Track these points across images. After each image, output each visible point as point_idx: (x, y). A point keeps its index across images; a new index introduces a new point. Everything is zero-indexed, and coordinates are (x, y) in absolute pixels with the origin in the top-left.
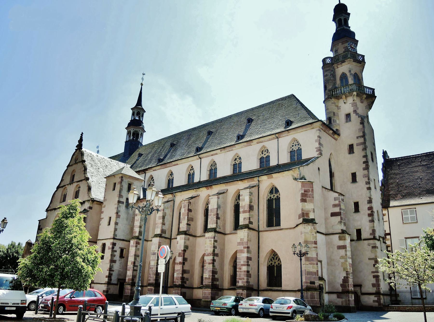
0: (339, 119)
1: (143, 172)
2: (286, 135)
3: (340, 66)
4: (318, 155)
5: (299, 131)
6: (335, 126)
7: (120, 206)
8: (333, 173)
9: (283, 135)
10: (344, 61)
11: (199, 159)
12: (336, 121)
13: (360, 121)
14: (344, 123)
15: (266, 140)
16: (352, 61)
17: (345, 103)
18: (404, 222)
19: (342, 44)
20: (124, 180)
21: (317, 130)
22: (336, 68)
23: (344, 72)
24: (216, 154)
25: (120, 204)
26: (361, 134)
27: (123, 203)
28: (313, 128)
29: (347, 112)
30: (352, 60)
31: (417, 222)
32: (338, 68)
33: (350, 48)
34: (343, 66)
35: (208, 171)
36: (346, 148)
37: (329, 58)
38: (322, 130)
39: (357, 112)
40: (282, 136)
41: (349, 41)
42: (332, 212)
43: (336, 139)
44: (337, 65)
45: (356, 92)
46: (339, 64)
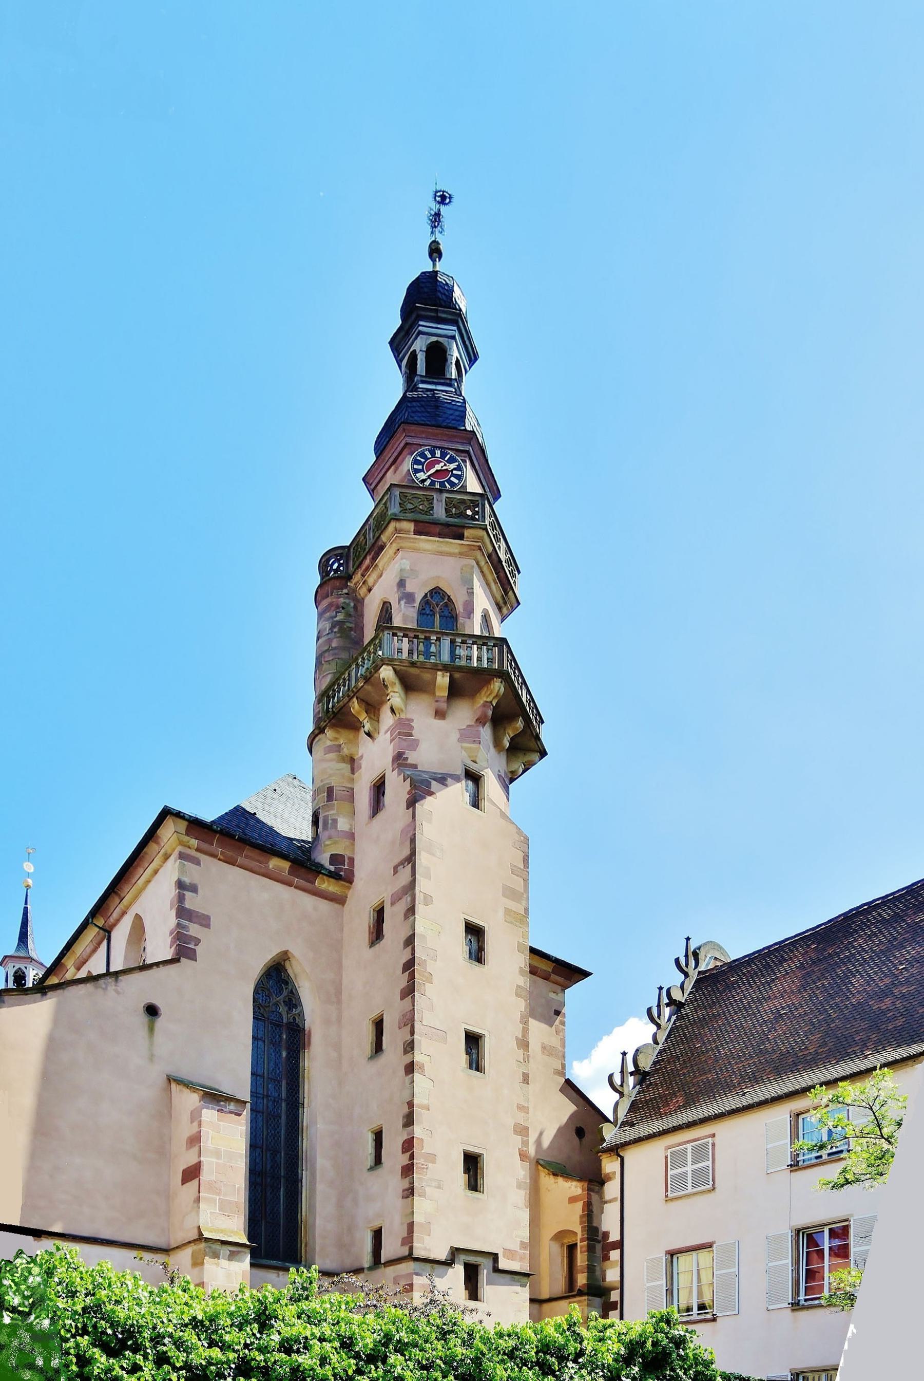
12: (335, 821)
41: (421, 446)
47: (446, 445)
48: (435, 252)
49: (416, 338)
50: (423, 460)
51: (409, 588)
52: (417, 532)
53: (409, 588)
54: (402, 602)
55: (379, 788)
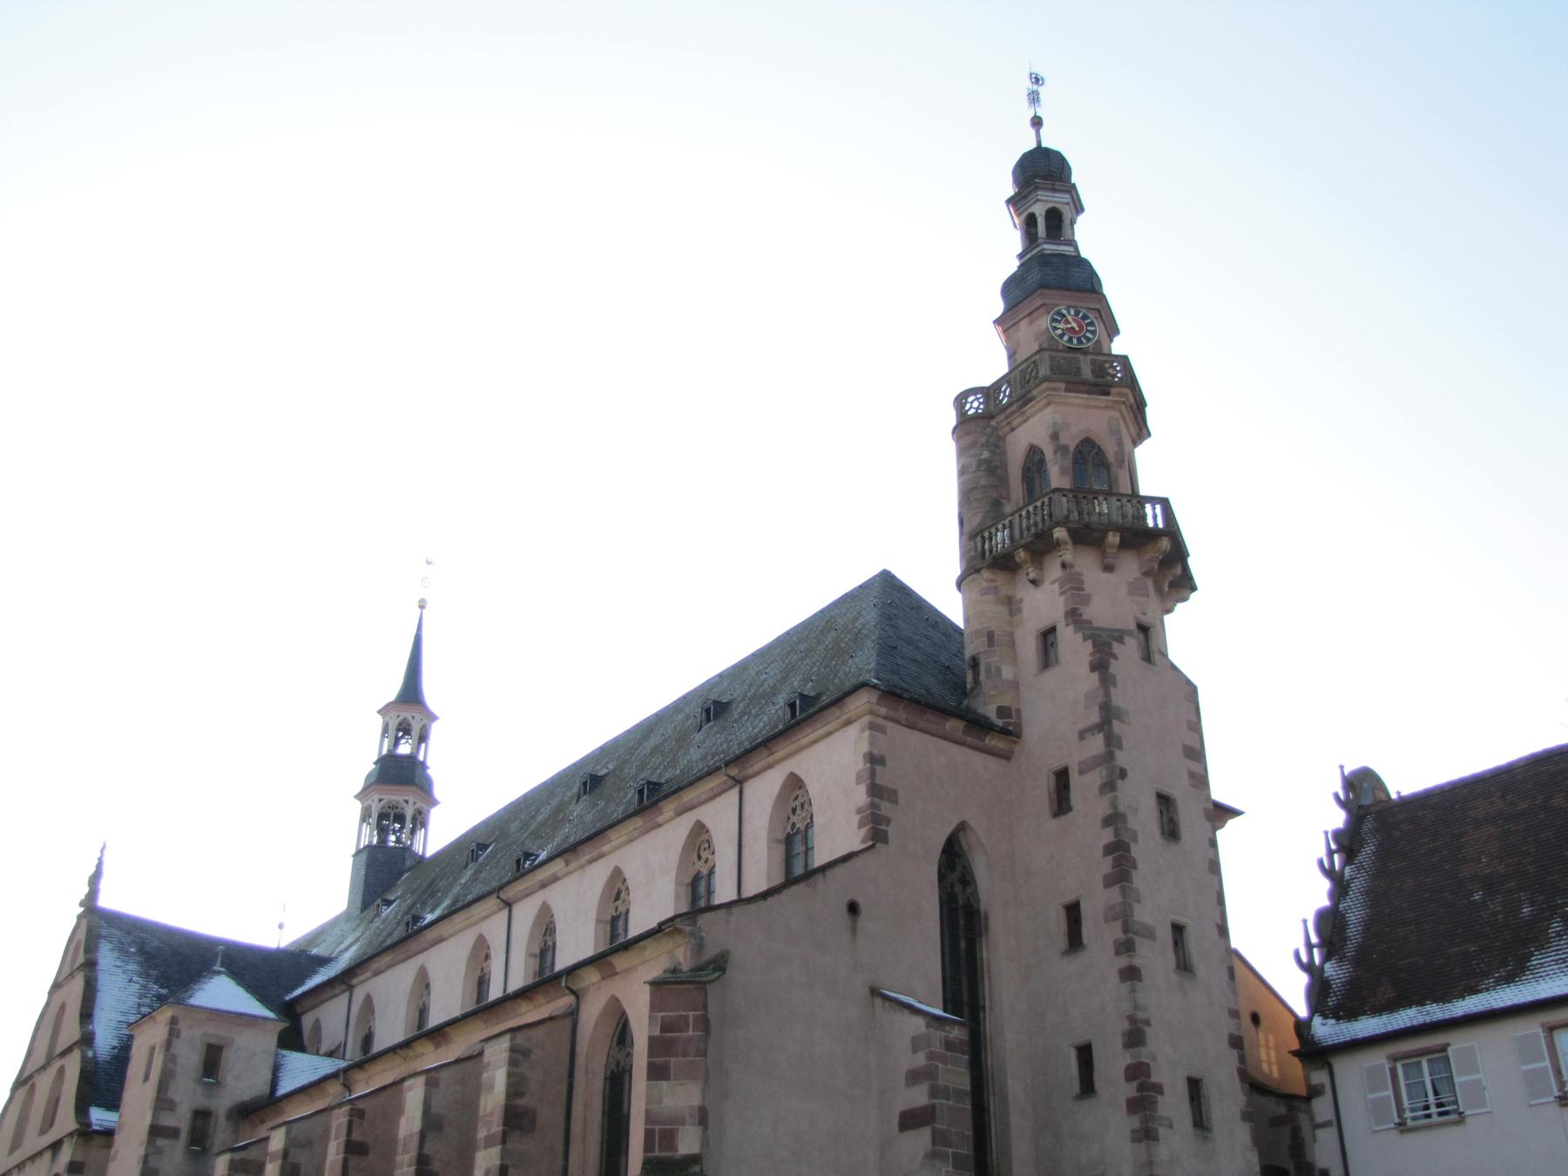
1: (344, 987)
2: (762, 763)
3: (1020, 420)
4: (863, 841)
5: (805, 741)
6: (993, 693)
7: (159, 1152)
9: (756, 767)
10: (1029, 396)
11: (501, 909)
12: (999, 670)
13: (1091, 658)
14: (1035, 676)
15: (704, 797)
17: (1034, 582)
19: (1031, 322)
20: (184, 1034)
21: (862, 730)
22: (1008, 433)
23: (1035, 442)
24: (555, 879)
25: (160, 1142)
26: (1094, 717)
27: (173, 1133)
28: (849, 722)
29: (1044, 624)
30: (1063, 386)
32: (1013, 430)
33: (1061, 336)
34: (1030, 422)
35: (533, 959)
36: (1043, 787)
37: (976, 395)
38: (890, 725)
39: (1081, 615)
40: (750, 771)
41: (1056, 305)
42: (905, 1107)
43: (1006, 756)
45: (1064, 529)
47: (1080, 304)
48: (1037, 122)
49: (1035, 202)
50: (1059, 319)
51: (1064, 440)
52: (1067, 390)
53: (1064, 440)
54: (1059, 454)
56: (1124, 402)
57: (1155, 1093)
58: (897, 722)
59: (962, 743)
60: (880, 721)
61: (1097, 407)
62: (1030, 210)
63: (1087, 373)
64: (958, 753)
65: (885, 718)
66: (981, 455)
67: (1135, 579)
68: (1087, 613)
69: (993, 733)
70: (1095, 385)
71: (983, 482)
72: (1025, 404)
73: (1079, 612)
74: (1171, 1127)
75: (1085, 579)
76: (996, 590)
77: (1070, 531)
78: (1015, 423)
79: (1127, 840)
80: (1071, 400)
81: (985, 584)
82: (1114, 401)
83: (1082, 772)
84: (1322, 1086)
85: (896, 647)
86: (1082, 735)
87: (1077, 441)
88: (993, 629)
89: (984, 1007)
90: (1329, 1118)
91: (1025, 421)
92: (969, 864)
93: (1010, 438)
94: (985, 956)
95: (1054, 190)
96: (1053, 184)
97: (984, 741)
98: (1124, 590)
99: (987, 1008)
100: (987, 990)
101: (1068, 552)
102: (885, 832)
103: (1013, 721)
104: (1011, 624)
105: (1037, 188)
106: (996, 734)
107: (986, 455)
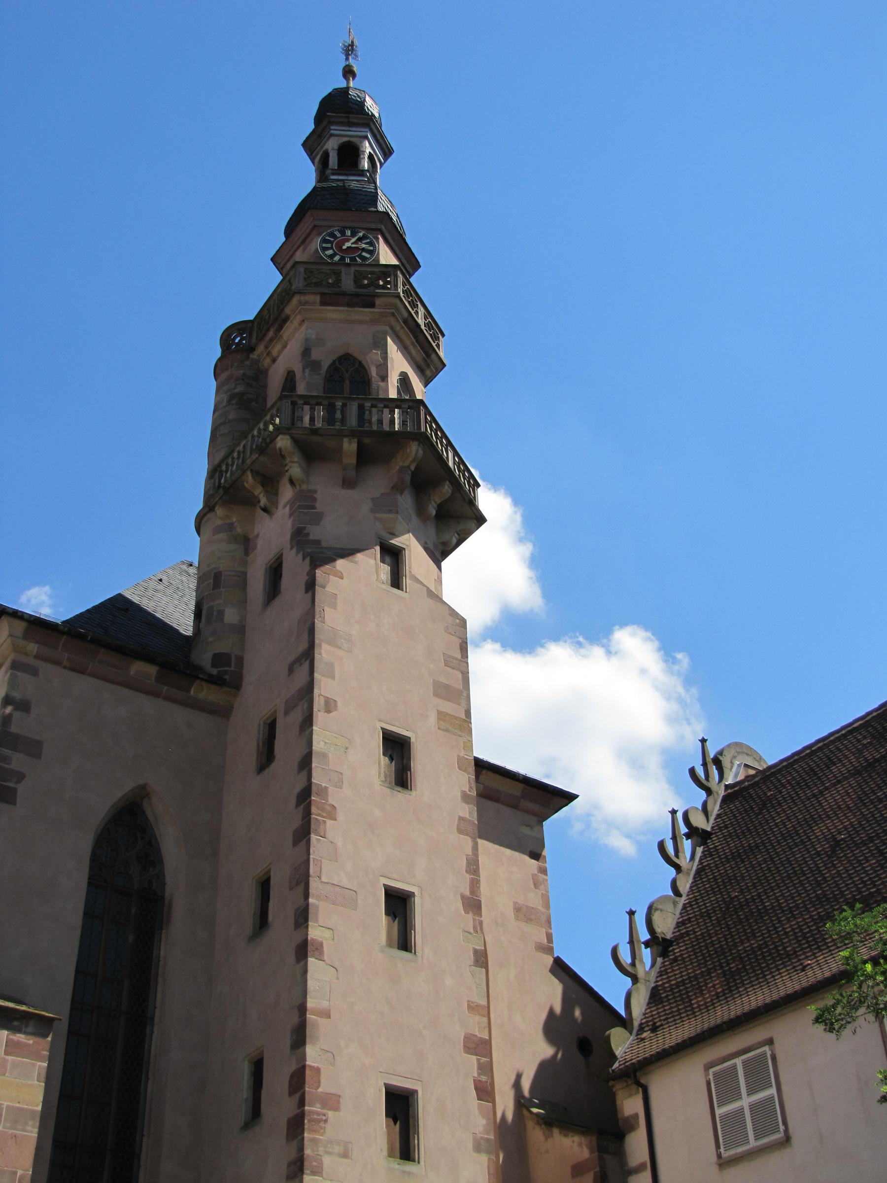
0: (246, 602)
3: (278, 347)
8: (170, 903)
10: (283, 316)
12: (221, 613)
13: (307, 577)
16: (313, 303)
17: (265, 510)
18: (722, 1150)
19: (304, 251)
22: (270, 366)
31: (787, 1139)
32: (274, 361)
34: (288, 347)
38: (46, 669)
41: (330, 227)
44: (266, 347)
45: (288, 437)
46: (271, 340)
47: (357, 225)
48: (348, 72)
49: (328, 139)
50: (332, 239)
51: (315, 355)
52: (323, 303)
53: (315, 355)
54: (307, 371)
55: (275, 572)
56: (393, 314)
57: (323, 1107)
58: (57, 663)
59: (155, 694)
60: (31, 661)
61: (361, 322)
62: (324, 149)
63: (348, 283)
64: (147, 705)
65: (37, 657)
66: (235, 388)
67: (383, 494)
68: (315, 532)
69: (198, 681)
70: (357, 295)
71: (231, 416)
72: (281, 327)
73: (306, 532)
74: (345, 1155)
75: (318, 496)
76: (231, 527)
77: (295, 441)
78: (275, 352)
79: (324, 785)
80: (329, 315)
81: (219, 522)
82: (380, 313)
83: (286, 713)
84: (636, 1116)
85: (127, 609)
86: (291, 669)
87: (335, 357)
88: (221, 569)
89: (153, 1019)
90: (641, 1160)
91: (284, 347)
92: (156, 840)
93: (271, 371)
94: (162, 953)
95: (351, 124)
96: (348, 117)
97: (188, 691)
98: (366, 507)
99: (156, 1020)
100: (159, 996)
101: (295, 465)
102: (14, 791)
103: (232, 669)
104: (245, 563)
105: (331, 123)
106: (204, 683)
107: (240, 389)
